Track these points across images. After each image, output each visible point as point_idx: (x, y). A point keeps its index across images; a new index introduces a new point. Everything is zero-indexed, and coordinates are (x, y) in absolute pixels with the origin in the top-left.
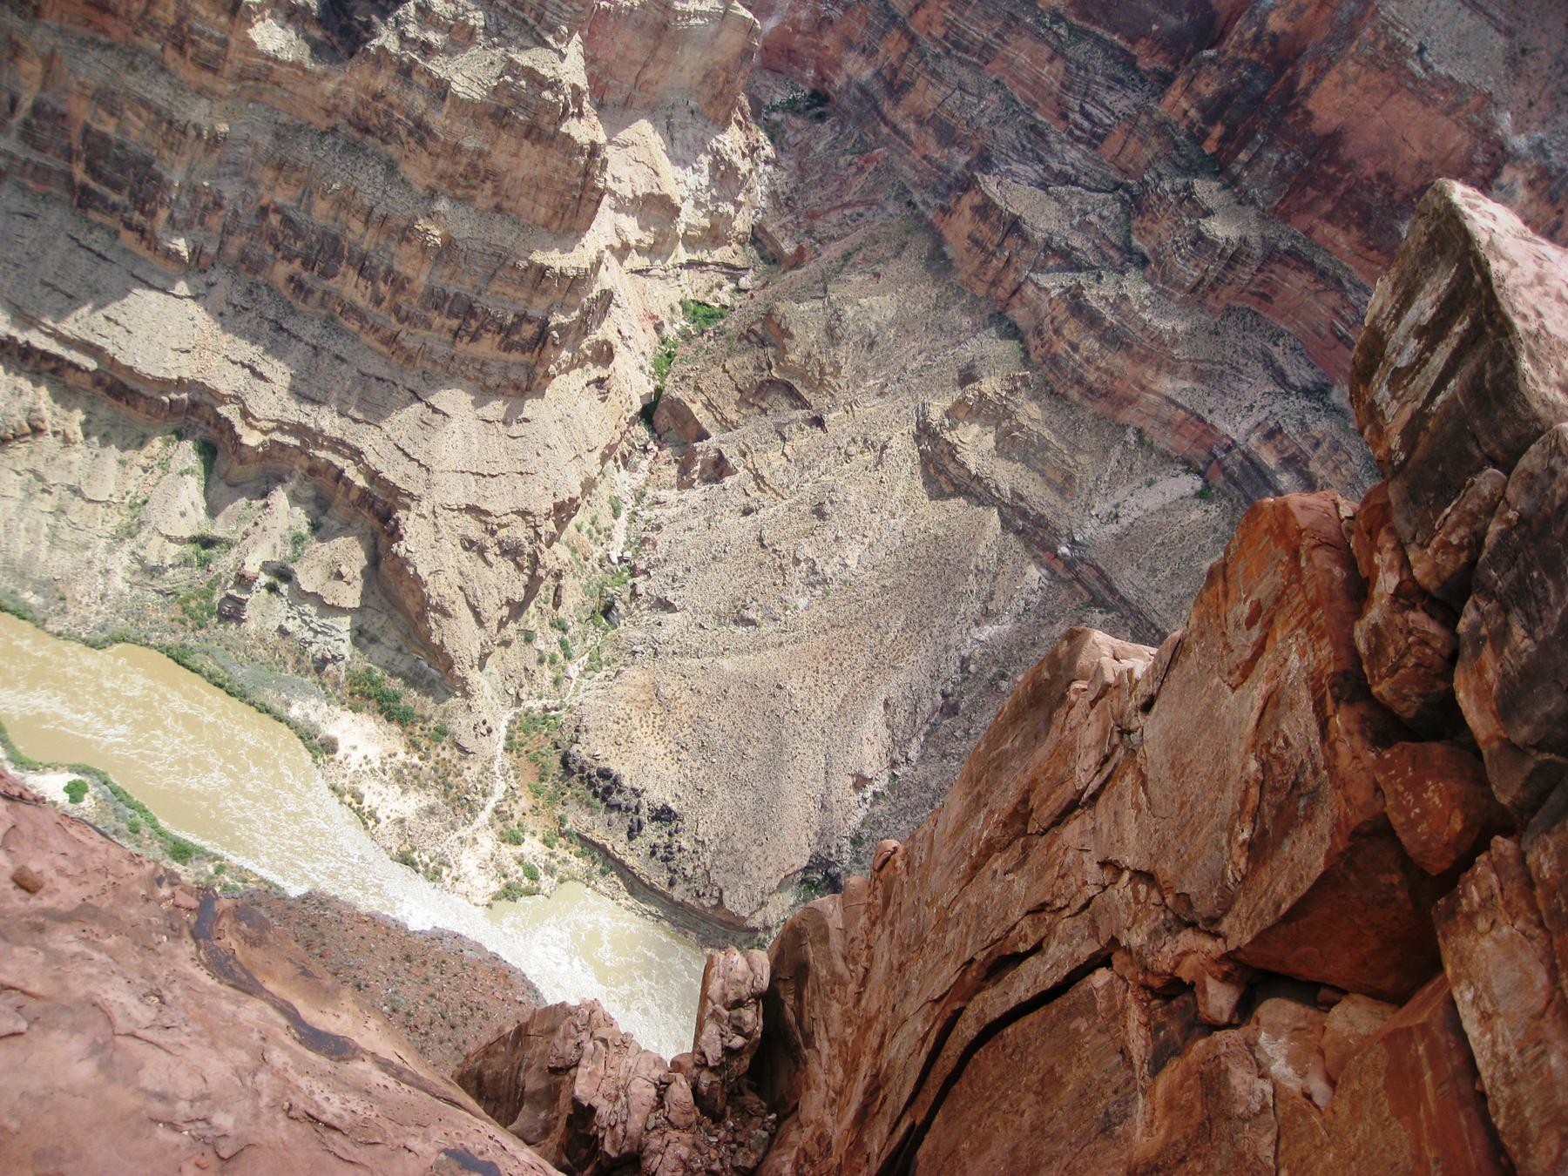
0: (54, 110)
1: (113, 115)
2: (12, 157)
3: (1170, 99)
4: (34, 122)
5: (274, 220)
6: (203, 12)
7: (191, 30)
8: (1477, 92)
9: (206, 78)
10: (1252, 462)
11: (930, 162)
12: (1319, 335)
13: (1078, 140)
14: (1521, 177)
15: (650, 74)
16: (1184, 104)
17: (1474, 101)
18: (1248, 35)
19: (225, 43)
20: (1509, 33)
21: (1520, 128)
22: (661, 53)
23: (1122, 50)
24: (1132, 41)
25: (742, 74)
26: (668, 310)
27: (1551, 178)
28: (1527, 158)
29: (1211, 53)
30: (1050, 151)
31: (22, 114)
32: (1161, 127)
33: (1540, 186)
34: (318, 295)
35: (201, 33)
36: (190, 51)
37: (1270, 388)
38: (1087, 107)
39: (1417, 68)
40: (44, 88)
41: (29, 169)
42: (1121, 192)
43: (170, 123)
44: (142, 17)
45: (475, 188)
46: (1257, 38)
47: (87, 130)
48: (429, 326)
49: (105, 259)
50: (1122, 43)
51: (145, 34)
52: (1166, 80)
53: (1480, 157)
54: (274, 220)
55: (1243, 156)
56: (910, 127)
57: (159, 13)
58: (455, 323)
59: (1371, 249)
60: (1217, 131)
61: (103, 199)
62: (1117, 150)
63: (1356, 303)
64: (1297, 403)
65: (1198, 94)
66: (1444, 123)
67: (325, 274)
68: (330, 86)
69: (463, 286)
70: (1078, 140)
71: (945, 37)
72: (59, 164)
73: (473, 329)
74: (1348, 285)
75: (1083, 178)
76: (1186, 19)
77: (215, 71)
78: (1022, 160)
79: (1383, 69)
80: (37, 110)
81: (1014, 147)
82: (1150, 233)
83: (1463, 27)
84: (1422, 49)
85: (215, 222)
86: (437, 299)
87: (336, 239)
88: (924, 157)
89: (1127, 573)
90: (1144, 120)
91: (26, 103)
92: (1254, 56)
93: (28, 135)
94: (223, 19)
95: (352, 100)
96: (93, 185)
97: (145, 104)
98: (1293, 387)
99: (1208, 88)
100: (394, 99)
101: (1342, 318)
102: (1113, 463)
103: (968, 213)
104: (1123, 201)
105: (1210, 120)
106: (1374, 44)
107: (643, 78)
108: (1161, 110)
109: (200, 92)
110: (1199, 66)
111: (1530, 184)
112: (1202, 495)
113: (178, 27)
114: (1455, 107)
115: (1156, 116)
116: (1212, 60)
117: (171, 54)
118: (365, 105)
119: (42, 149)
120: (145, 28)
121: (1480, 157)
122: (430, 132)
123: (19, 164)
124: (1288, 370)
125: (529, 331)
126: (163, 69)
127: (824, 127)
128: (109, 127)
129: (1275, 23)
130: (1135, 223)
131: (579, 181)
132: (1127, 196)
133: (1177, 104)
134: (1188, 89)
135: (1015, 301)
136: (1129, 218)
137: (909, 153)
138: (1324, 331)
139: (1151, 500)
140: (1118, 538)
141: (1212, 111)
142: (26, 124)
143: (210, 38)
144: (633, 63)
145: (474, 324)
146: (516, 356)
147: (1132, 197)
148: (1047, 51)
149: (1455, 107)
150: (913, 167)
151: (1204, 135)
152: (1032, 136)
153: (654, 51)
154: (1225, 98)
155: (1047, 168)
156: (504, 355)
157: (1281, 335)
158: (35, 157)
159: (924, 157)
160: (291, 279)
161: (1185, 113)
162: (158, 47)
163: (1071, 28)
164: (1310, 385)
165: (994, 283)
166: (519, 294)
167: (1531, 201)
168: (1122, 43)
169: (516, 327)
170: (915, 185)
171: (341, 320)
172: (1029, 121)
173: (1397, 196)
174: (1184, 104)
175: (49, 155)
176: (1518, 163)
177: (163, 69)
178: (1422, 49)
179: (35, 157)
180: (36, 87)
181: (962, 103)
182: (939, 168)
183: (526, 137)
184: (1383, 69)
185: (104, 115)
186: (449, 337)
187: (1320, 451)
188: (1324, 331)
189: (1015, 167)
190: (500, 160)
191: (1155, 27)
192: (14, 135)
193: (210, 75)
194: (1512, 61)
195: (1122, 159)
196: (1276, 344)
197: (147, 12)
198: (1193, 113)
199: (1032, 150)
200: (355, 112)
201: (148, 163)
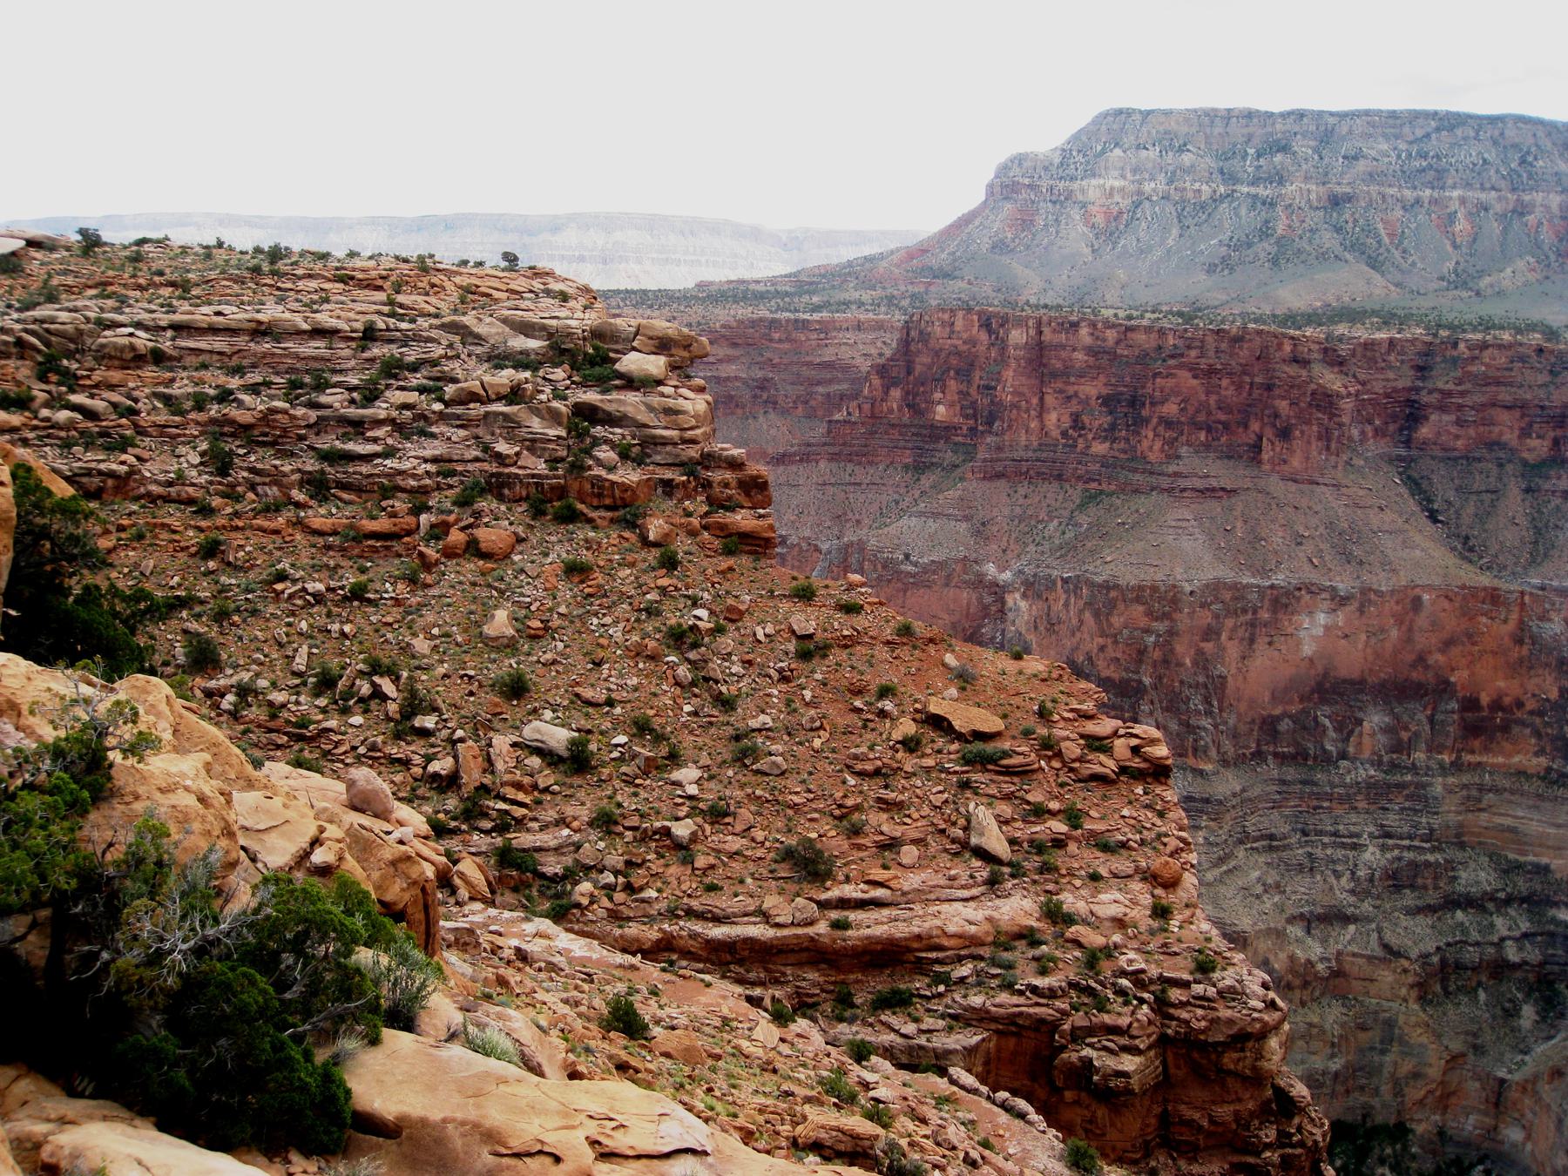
8: (957, 561)
14: (1017, 596)
17: (959, 568)
20: (967, 518)
21: (1002, 569)
27: (1033, 584)
28: (1013, 582)
39: (910, 568)
53: (988, 600)
66: (951, 593)
79: (889, 581)
83: (932, 530)
84: (907, 556)
106: (875, 570)
111: (1024, 596)
121: (988, 600)
178: (907, 556)
184: (889, 581)
194: (978, 533)
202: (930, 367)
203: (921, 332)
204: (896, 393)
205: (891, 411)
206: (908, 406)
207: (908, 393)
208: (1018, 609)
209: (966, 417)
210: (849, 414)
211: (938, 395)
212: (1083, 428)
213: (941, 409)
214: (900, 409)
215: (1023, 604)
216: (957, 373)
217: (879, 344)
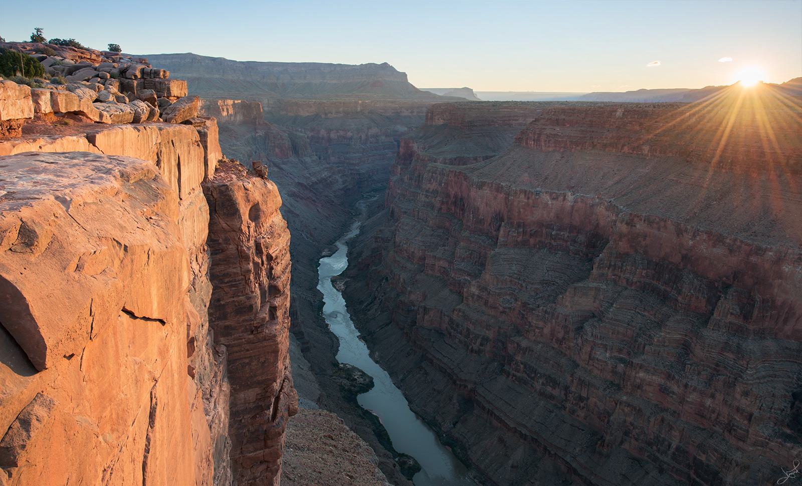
0: (683, 450)
1: (704, 454)
4: (677, 453)
7: (733, 425)
9: (741, 444)
19: (748, 431)
35: (738, 427)
40: (680, 442)
41: (675, 470)
43: (726, 459)
47: (695, 458)
51: (717, 426)
57: (721, 418)
77: (744, 441)
80: (678, 449)
91: (674, 446)
94: (746, 422)
97: (716, 450)
109: (738, 449)
117: (726, 434)
120: (717, 424)
126: (724, 439)
128: (703, 458)
142: (674, 453)
143: (741, 429)
162: (722, 431)
177: (724, 439)
180: (678, 441)
185: (701, 454)
192: (669, 457)
193: (742, 443)
197: (717, 418)
201: (717, 473)
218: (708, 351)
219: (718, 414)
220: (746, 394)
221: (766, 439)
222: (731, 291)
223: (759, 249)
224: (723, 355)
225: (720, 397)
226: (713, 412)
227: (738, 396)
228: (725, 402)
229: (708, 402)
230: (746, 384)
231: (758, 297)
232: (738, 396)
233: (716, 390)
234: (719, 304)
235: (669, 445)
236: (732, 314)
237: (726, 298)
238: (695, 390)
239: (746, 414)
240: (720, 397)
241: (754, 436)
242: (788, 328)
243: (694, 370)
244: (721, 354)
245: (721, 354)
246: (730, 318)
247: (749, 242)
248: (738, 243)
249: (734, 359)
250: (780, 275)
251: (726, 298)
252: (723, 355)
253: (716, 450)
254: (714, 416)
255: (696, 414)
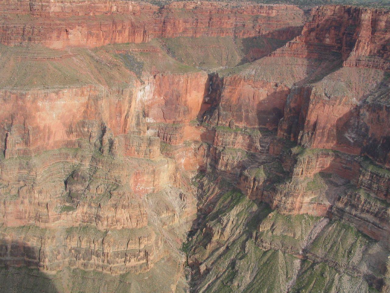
0: (16, 246)
2: (10, 261)
3: (278, 133)
4: (13, 250)
5: (73, 251)
6: (41, 210)
10: (339, 209)
11: (232, 174)
12: (340, 170)
13: (263, 153)
15: (156, 183)
16: (282, 133)
18: (288, 111)
22: (156, 177)
23: (264, 128)
24: (265, 125)
25: (178, 174)
26: (182, 236)
29: (282, 119)
30: (258, 159)
31: (9, 250)
32: (279, 140)
33: (370, 110)
34: (90, 265)
36: (40, 220)
37: (335, 188)
38: (262, 144)
42: (276, 160)
44: (28, 217)
45: (115, 225)
46: (290, 110)
48: (118, 263)
49: (37, 277)
50: (263, 127)
52: (276, 130)
54: (73, 251)
55: (299, 138)
56: (223, 169)
58: (123, 259)
59: (340, 144)
60: (292, 135)
61: (33, 262)
62: (272, 151)
63: (344, 158)
64: (342, 188)
65: (284, 129)
67: (89, 260)
68: (74, 215)
69: (122, 249)
70: (263, 153)
71: (222, 144)
72: (22, 258)
73: (128, 259)
74: (340, 155)
75: (268, 161)
76: (274, 114)
77: (48, 222)
78: (253, 163)
81: (250, 162)
82: (287, 166)
85: (59, 257)
86: (117, 255)
87: (88, 250)
88: (230, 174)
89: (320, 251)
90: (275, 141)
92: (292, 115)
93: (12, 254)
94: (46, 210)
95: (81, 216)
96: (30, 260)
98: (341, 185)
99: (285, 127)
100: (89, 212)
101: (343, 163)
102: (304, 225)
103: (243, 181)
104: (278, 162)
105: (290, 134)
107: (154, 184)
108: (278, 137)
110: (281, 123)
111: (368, 110)
112: (330, 223)
113: (36, 216)
114: (340, 103)
115: (277, 139)
116: (283, 120)
118: (84, 216)
119: (16, 256)
122: (100, 216)
123: (12, 262)
124: (337, 182)
125: (142, 254)
127: (205, 178)
129: (292, 105)
130: (283, 165)
131: (139, 213)
132: (278, 160)
133: (281, 134)
134: (281, 130)
135: (263, 197)
136: (281, 165)
137: (226, 174)
138: (341, 168)
139: (318, 230)
140: (313, 243)
141: (289, 131)
142: (11, 252)
144: (151, 182)
145: (128, 258)
146: (142, 262)
147: (280, 159)
148: (247, 137)
149: (340, 103)
150: (228, 177)
151: (290, 137)
152: (253, 157)
153: (154, 177)
154: (290, 127)
155: (259, 163)
156: (139, 263)
157: (331, 175)
158: (16, 259)
159: (230, 174)
160: (82, 264)
161: (283, 135)
163: (250, 129)
164: (344, 183)
165: (257, 195)
166: (136, 246)
167: (370, 114)
168: (263, 127)
169: (139, 255)
170: (231, 181)
171: (97, 269)
172: (251, 154)
173: (340, 129)
174: (282, 133)
175: (18, 257)
176: (362, 107)
179: (16, 259)
181: (233, 157)
182: (235, 174)
183: (122, 208)
186: (124, 264)
187: (353, 198)
188: (341, 168)
189: (252, 166)
190: (118, 216)
191: (268, 120)
192: (9, 255)
195: (275, 152)
196: (331, 177)
197: (29, 215)
198: (285, 134)
199: (254, 160)
200: (83, 219)
202: (325, 25)
203: (323, 13)
204: (313, 34)
205: (310, 40)
206: (317, 38)
207: (317, 34)
208: (365, 115)
209: (338, 43)
210: (296, 40)
211: (327, 35)
212: (387, 50)
213: (328, 40)
214: (314, 39)
215: (367, 114)
216: (335, 28)
217: (293, 15)
218: (10, 174)
219: (29, 213)
220: (40, 192)
221: (58, 215)
222: (13, 128)
223: (22, 95)
224: (20, 173)
225: (26, 201)
226: (26, 212)
227: (37, 195)
228: (30, 203)
229: (21, 208)
230: (39, 186)
231: (30, 127)
232: (37, 195)
233: (23, 198)
234: (8, 139)
235: (7, 248)
236: (18, 143)
237: (11, 134)
238: (10, 204)
239: (44, 205)
240: (26, 201)
241: (52, 217)
242: (51, 141)
243: (6, 190)
244: (19, 172)
245: (19, 172)
246: (18, 147)
247: (15, 91)
248: (8, 94)
249: (27, 173)
250: (37, 109)
251: (11, 134)
252: (20, 173)
253: (35, 237)
254: (27, 215)
255: (16, 219)
